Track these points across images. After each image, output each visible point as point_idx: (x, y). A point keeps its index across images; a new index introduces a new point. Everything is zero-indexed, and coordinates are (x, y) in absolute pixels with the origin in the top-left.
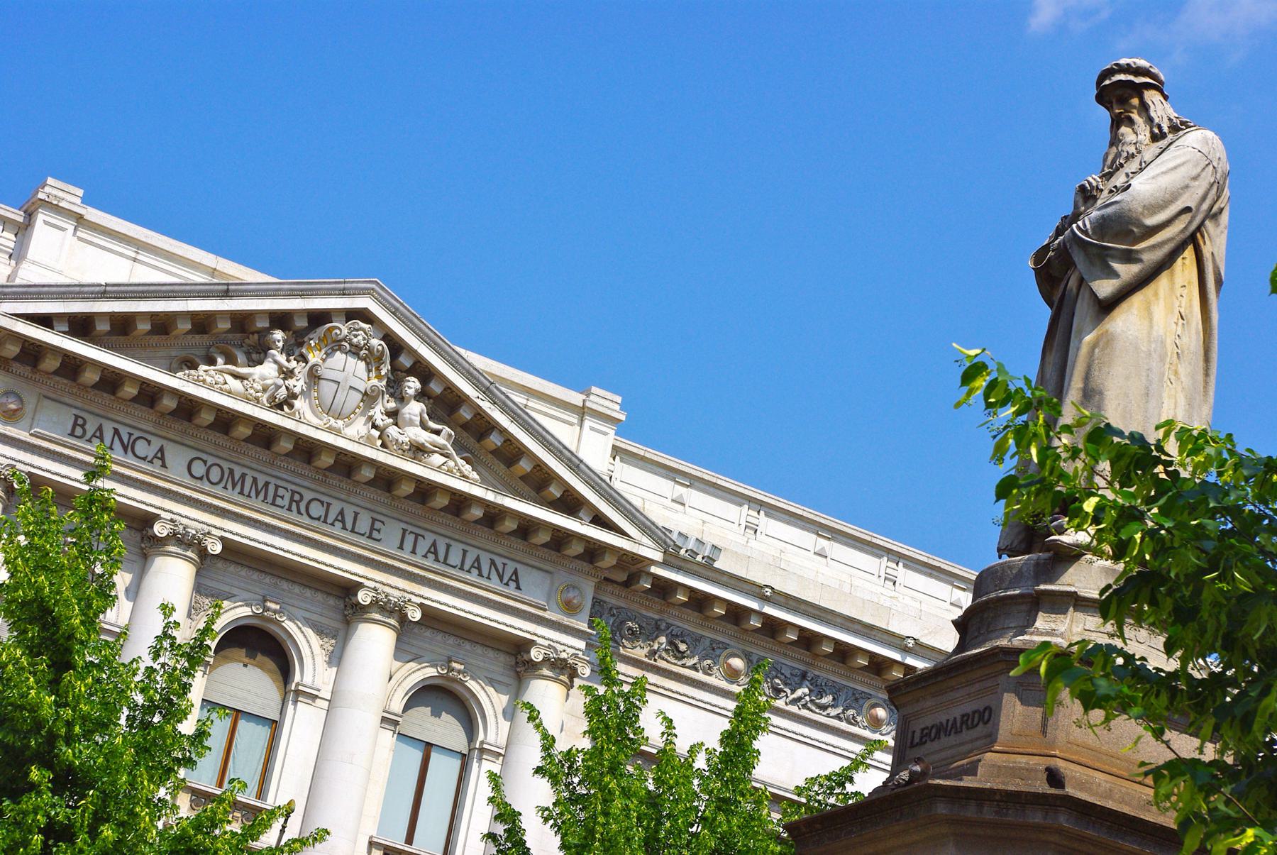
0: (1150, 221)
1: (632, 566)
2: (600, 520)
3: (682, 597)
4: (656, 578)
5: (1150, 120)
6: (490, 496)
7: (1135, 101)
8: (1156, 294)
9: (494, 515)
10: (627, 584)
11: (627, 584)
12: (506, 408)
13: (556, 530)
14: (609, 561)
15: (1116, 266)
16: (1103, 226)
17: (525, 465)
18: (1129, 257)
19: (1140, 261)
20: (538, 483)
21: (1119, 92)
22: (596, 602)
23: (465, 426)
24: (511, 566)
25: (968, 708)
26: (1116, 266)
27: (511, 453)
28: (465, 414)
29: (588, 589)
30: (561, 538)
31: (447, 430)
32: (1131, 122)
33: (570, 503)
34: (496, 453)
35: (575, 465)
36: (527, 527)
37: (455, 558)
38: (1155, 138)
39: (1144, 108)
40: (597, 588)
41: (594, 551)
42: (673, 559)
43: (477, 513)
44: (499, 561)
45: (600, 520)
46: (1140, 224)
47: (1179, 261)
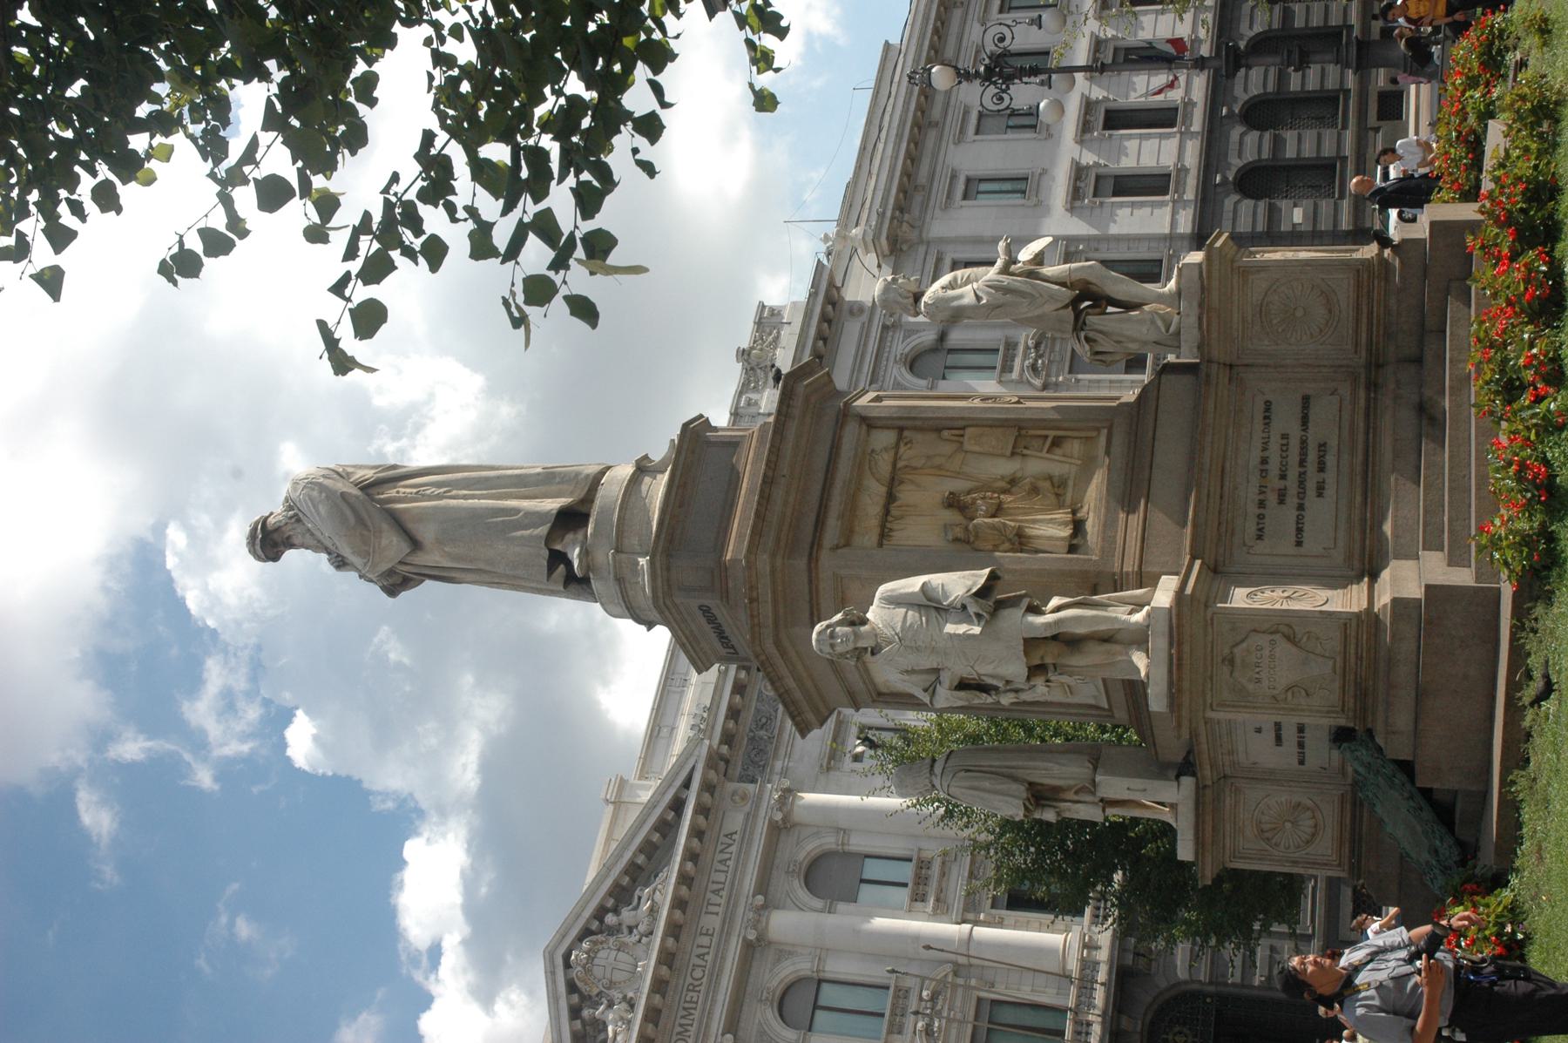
0: (352, 520)
2: (687, 785)
4: (721, 743)
6: (678, 859)
9: (691, 856)
10: (727, 762)
11: (727, 762)
13: (697, 811)
14: (712, 775)
17: (656, 837)
20: (666, 828)
22: (741, 779)
23: (634, 880)
24: (722, 839)
25: (703, 621)
27: (648, 848)
28: (626, 880)
29: (731, 786)
30: (701, 810)
31: (637, 892)
33: (677, 805)
34: (649, 858)
35: (652, 805)
36: (697, 833)
37: (721, 877)
40: (731, 780)
41: (708, 787)
43: (689, 865)
44: (720, 847)
45: (687, 785)
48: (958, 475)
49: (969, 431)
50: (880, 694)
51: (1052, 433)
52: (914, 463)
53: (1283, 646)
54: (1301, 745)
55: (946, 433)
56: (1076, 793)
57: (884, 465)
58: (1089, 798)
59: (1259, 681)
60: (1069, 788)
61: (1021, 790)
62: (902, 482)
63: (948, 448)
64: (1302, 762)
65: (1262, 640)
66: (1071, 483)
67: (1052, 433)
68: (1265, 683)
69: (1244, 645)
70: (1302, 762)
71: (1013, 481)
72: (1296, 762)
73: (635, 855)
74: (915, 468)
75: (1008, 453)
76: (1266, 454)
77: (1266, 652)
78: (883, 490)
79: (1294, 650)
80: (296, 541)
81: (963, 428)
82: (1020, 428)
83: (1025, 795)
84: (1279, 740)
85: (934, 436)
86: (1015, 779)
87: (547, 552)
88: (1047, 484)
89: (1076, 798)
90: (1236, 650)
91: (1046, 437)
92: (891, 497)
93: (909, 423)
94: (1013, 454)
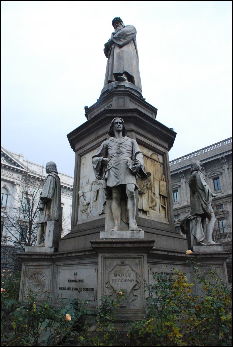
1: (26, 173)
2: (22, 168)
3: (32, 176)
4: (29, 175)
5: (122, 26)
6: (9, 165)
7: (119, 23)
8: (129, 46)
9: (9, 167)
12: (10, 155)
15: (122, 40)
16: (119, 35)
17: (13, 162)
18: (124, 39)
19: (126, 39)
20: (15, 164)
21: (116, 22)
24: (12, 173)
26: (122, 40)
30: (17, 170)
31: (3, 158)
32: (119, 26)
33: (19, 166)
34: (9, 160)
35: (19, 162)
37: (5, 172)
38: (123, 28)
39: (121, 24)
41: (22, 171)
42: (30, 172)
44: (10, 173)
45: (22, 168)
46: (126, 34)
47: (130, 44)
48: (154, 178)
49: (165, 183)
50: (81, 156)
51: (166, 207)
52: (156, 166)
53: (132, 285)
54: (69, 289)
55: (164, 176)
56: (48, 214)
57: (155, 157)
58: (46, 219)
59: (116, 275)
60: (49, 212)
61: (50, 196)
62: (152, 161)
63: (160, 176)
64: (61, 288)
65: (133, 276)
66: (155, 212)
67: (166, 207)
68: (114, 278)
69: (130, 269)
70: (61, 288)
71: (154, 194)
72: (60, 287)
73: (10, 158)
74: (155, 166)
75: (161, 193)
76: (174, 274)
77: (128, 278)
78: (149, 155)
79: (130, 290)
80: (118, 28)
81: (165, 181)
82: (167, 198)
83: (48, 198)
84: (70, 281)
85: (163, 173)
86: (53, 195)
87: (122, 72)
88: (154, 205)
89: (47, 214)
90: (128, 266)
91: (165, 205)
92: (148, 157)
93: (165, 166)
94: (160, 195)
